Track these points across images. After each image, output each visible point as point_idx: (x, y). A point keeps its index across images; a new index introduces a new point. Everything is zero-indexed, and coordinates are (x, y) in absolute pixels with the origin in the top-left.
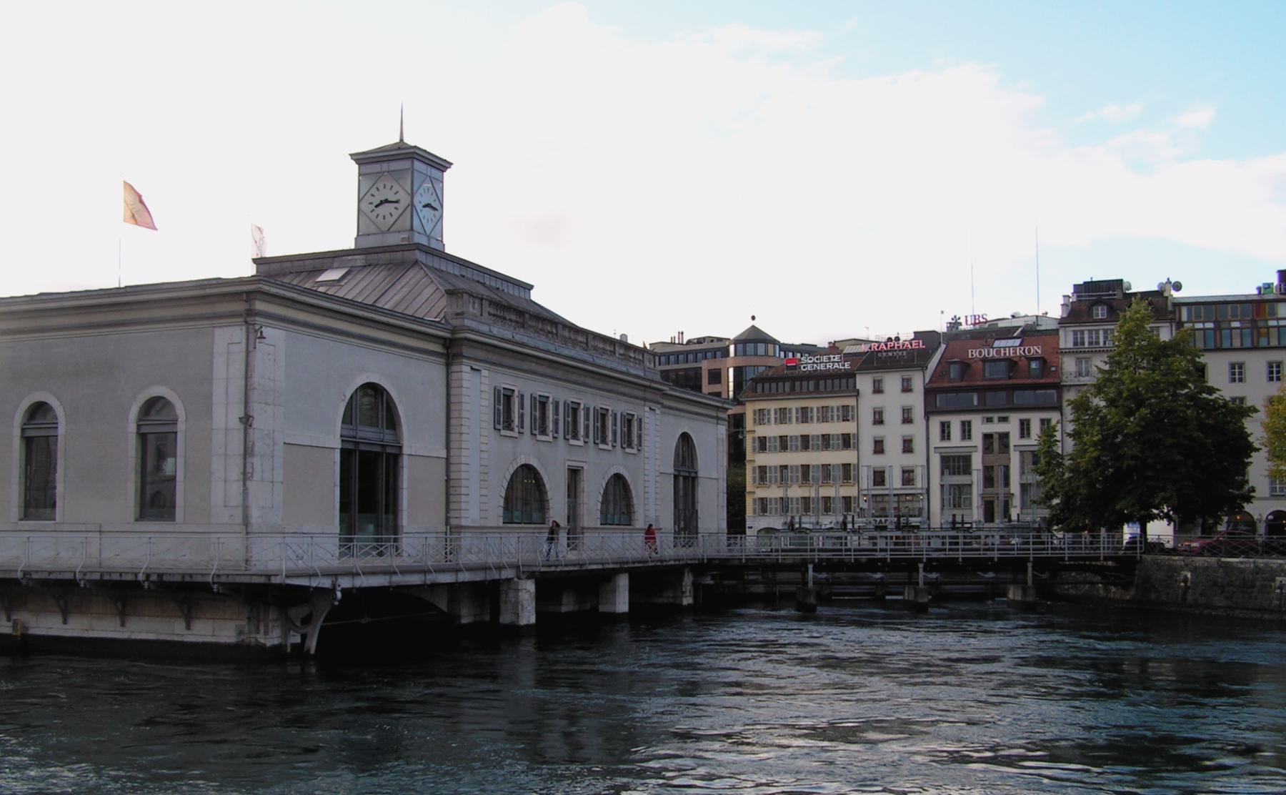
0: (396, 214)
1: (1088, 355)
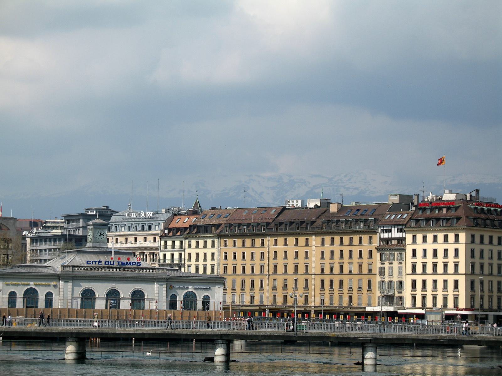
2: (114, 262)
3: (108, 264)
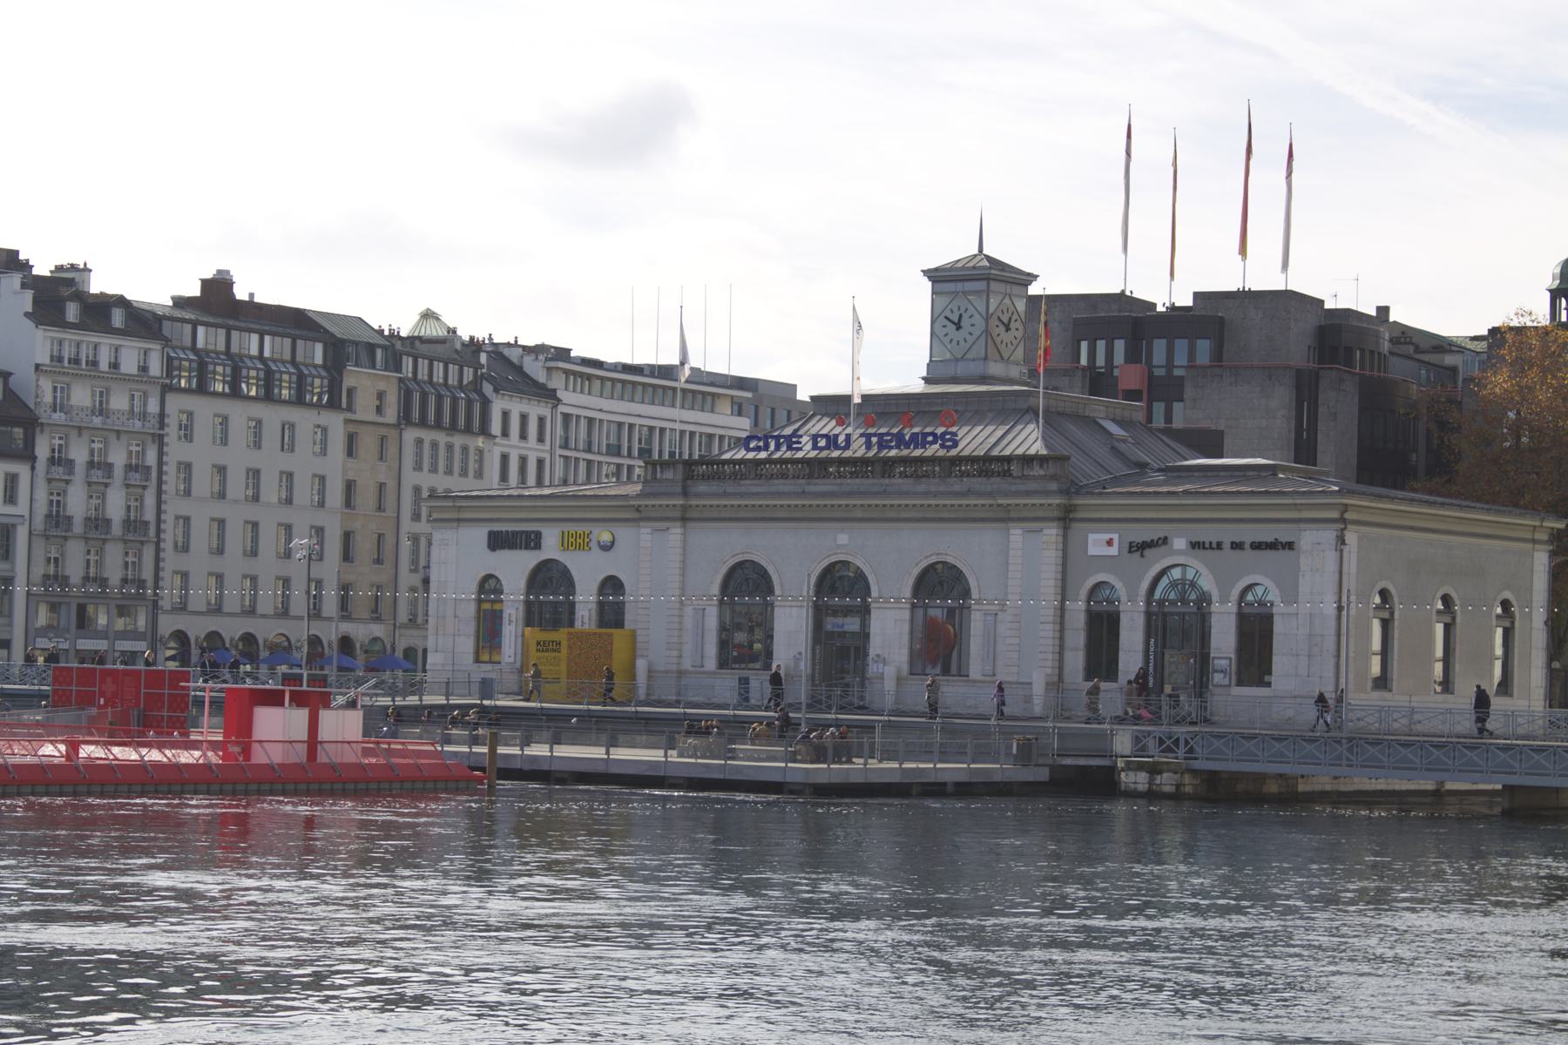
0: (971, 339)
1: (66, 379)
2: (848, 437)
3: (827, 447)
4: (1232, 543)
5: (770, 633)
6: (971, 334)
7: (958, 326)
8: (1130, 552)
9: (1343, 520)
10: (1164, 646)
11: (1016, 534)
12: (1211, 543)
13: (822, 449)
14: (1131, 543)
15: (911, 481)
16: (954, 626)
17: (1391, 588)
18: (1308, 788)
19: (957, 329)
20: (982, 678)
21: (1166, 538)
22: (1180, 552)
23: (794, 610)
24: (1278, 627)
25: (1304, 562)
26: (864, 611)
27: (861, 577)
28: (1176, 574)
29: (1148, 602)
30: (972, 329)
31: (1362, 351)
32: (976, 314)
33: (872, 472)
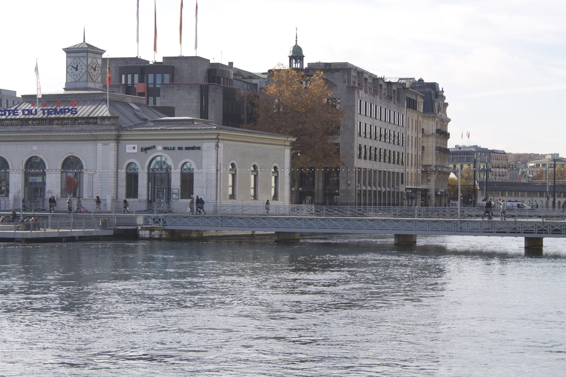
0: (81, 74)
2: (36, 110)
3: (28, 114)
4: (178, 147)
5: (8, 183)
6: (81, 72)
7: (77, 69)
8: (141, 151)
9: (218, 139)
10: (154, 185)
11: (100, 145)
12: (171, 148)
13: (26, 115)
14: (142, 148)
15: (60, 126)
16: (77, 179)
17: (235, 163)
18: (207, 235)
19: (76, 70)
20: (88, 198)
21: (154, 146)
22: (160, 151)
23: (17, 174)
24: (195, 178)
25: (204, 154)
26: (44, 174)
27: (42, 161)
28: (158, 159)
29: (148, 169)
30: (82, 70)
31: (224, 78)
32: (83, 65)
33: (45, 123)
